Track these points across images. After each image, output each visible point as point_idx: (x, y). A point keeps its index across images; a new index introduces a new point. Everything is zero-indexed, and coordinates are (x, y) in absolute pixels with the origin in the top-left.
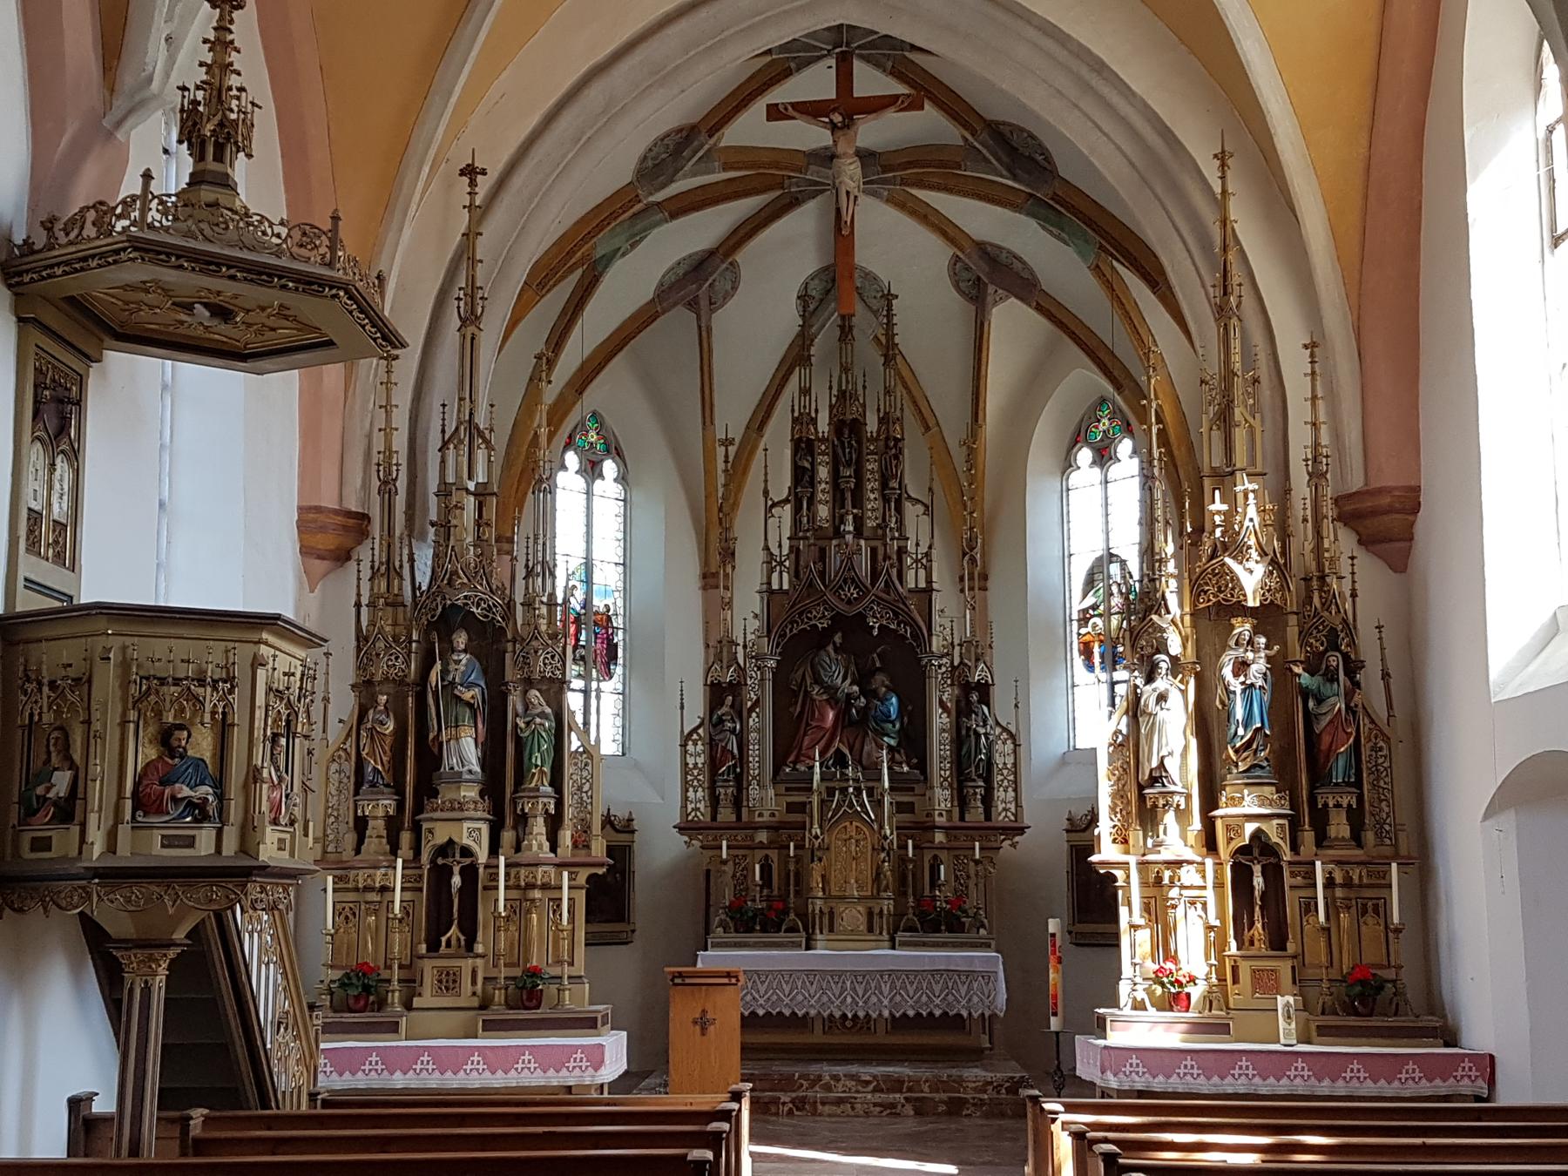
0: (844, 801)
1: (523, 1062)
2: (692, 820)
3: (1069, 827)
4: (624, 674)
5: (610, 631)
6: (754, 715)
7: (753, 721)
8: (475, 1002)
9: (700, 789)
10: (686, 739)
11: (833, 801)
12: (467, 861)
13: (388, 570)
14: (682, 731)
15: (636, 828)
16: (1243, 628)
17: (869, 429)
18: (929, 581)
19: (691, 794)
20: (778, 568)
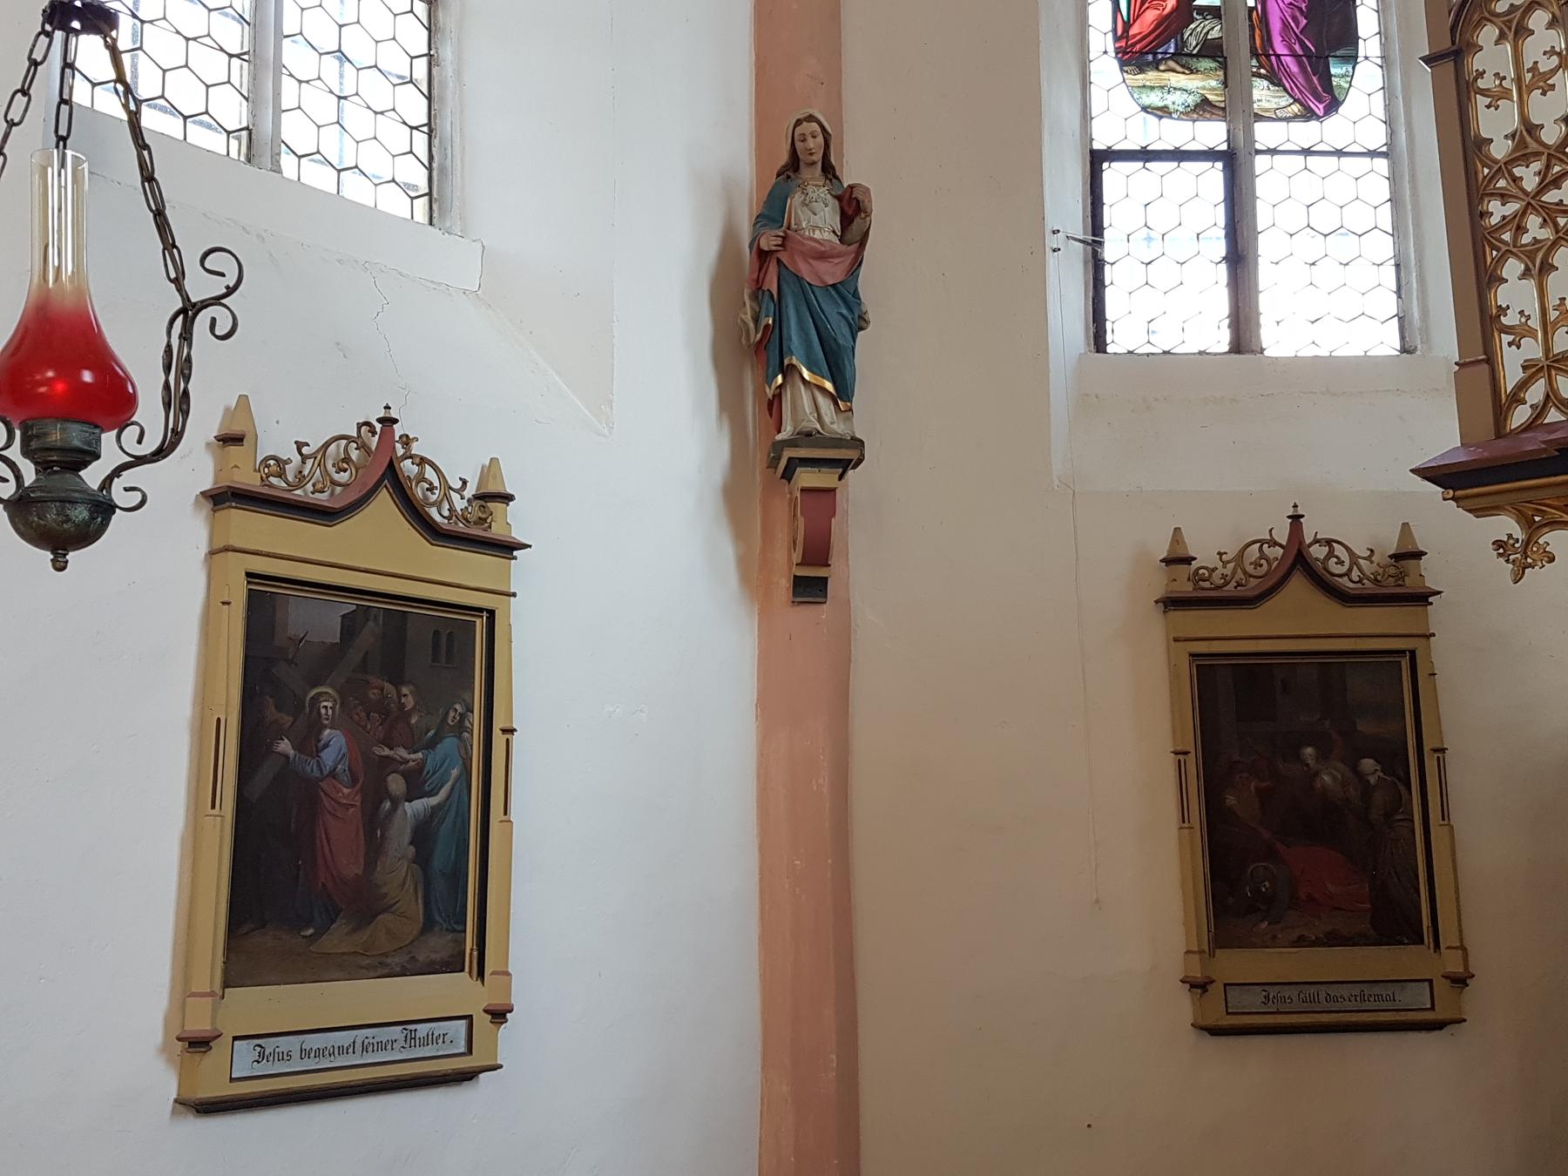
2: (1529, 427)
4: (1388, 89)
15: (1431, 584)
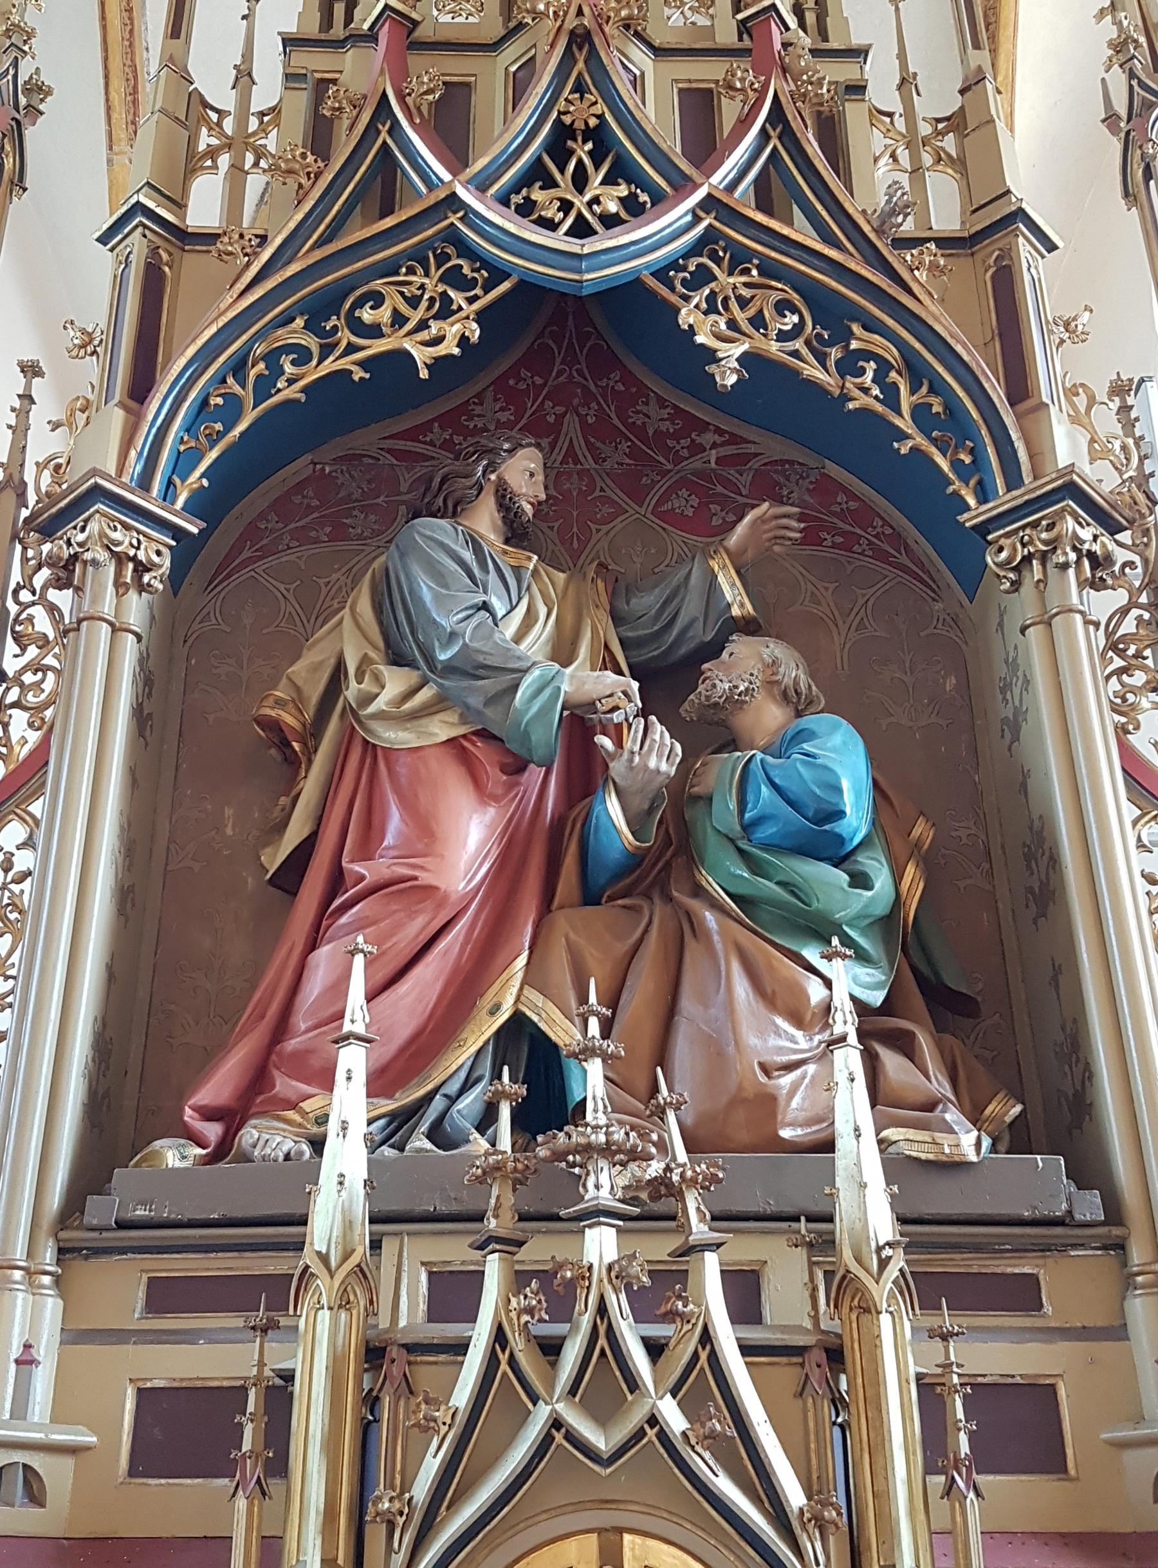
0: (551, 1349)
11: (461, 1348)
20: (224, 160)
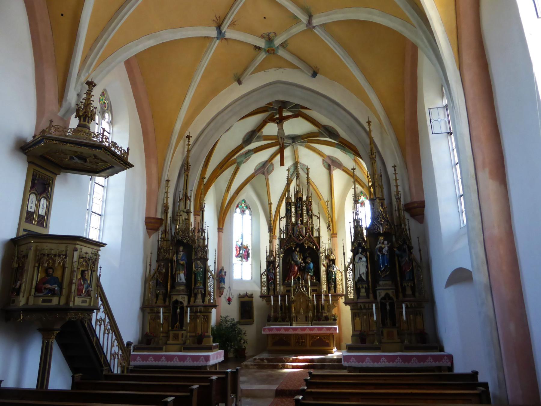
1: (188, 359)
3: (325, 294)
5: (248, 250)
6: (278, 268)
7: (278, 270)
8: (182, 343)
9: (265, 287)
10: (261, 275)
12: (181, 305)
13: (165, 232)
14: (261, 273)
16: (381, 238)
17: (304, 199)
18: (319, 235)
19: (263, 288)
